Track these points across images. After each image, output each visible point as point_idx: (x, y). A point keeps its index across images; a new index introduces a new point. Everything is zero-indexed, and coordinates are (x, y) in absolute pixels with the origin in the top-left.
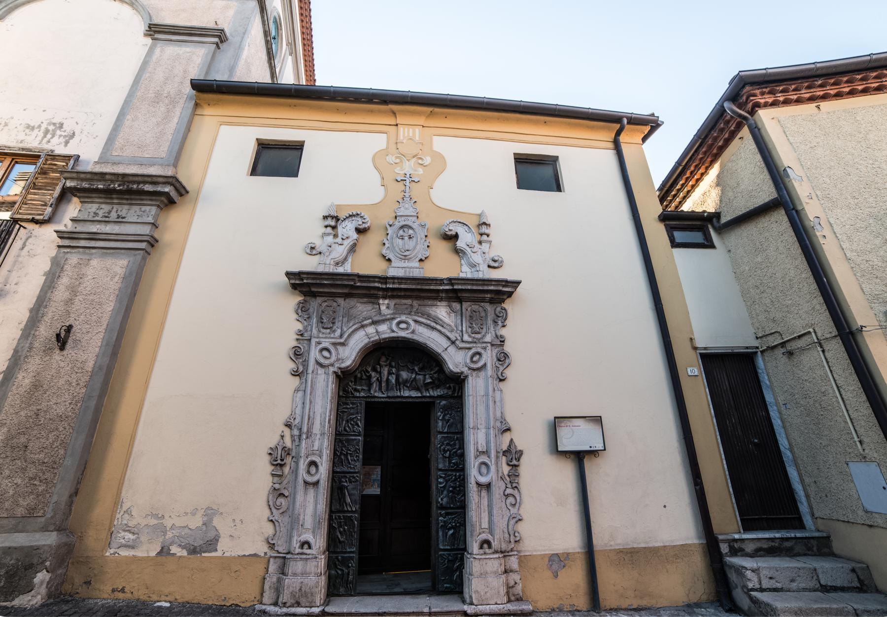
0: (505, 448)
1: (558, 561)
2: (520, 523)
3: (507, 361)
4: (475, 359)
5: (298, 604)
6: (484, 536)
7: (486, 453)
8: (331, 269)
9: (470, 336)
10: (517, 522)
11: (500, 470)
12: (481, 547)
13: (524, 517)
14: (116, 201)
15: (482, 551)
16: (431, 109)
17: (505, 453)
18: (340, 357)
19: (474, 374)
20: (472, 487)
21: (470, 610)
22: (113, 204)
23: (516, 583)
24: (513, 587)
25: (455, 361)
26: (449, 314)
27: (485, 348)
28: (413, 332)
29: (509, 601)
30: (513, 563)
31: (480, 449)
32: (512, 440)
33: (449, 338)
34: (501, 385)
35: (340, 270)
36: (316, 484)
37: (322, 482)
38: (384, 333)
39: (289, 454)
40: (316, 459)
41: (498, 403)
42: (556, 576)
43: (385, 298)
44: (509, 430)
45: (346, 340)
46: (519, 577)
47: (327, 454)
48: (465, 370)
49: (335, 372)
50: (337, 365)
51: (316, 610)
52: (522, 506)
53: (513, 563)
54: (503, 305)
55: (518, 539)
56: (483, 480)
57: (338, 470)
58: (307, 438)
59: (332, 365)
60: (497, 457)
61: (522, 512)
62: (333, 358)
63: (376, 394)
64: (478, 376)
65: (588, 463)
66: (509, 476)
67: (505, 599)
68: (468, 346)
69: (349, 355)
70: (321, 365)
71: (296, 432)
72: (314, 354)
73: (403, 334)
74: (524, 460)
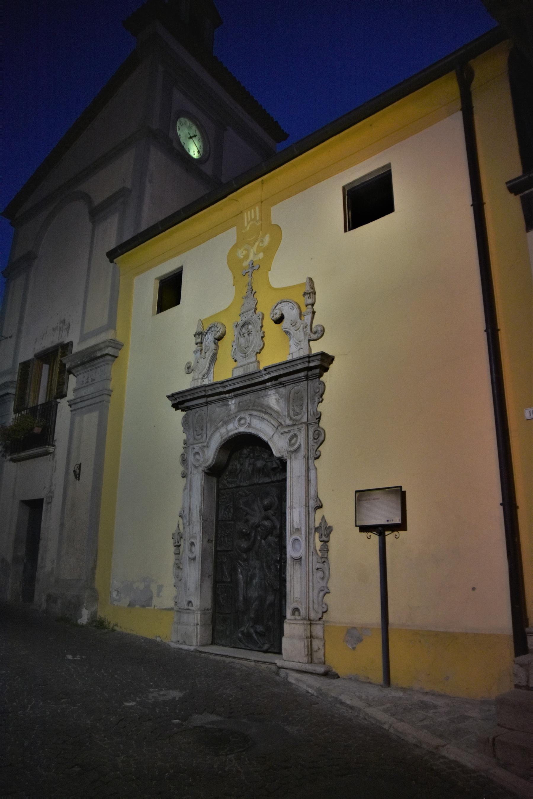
0: (317, 525)
1: (354, 635)
2: (327, 595)
3: (321, 438)
4: (293, 441)
5: (184, 643)
6: (295, 605)
7: (298, 530)
8: (199, 383)
9: (291, 419)
10: (325, 595)
11: (312, 545)
12: (293, 614)
13: (332, 589)
14: (89, 369)
15: (293, 617)
16: (259, 180)
17: (317, 530)
18: (206, 457)
19: (293, 456)
20: (289, 561)
21: (279, 663)
22: (88, 371)
23: (319, 649)
24: (316, 651)
25: (279, 445)
26: (277, 401)
27: (300, 430)
28: (249, 425)
29: (311, 662)
30: (318, 630)
31: (296, 527)
32: (323, 517)
33: (274, 426)
34: (316, 462)
35: (206, 382)
36: (194, 559)
37: (197, 557)
38: (231, 431)
39: (181, 538)
40: (193, 540)
41: (313, 482)
42: (354, 648)
43: (232, 398)
44: (321, 507)
45: (208, 443)
46: (322, 643)
47: (199, 535)
48: (285, 455)
49: (203, 471)
50: (203, 465)
51: (192, 648)
52: (330, 580)
53: (318, 630)
54: (321, 379)
55: (325, 610)
56: (296, 555)
57: (219, 549)
58: (189, 524)
59: (200, 466)
60: (308, 534)
61: (329, 585)
62: (202, 459)
63: (241, 484)
64: (296, 458)
65: (390, 537)
66: (320, 551)
67: (306, 659)
68: (287, 430)
69: (210, 455)
70: (196, 467)
71: (185, 521)
72: (191, 459)
73: (242, 429)
74: (333, 536)
